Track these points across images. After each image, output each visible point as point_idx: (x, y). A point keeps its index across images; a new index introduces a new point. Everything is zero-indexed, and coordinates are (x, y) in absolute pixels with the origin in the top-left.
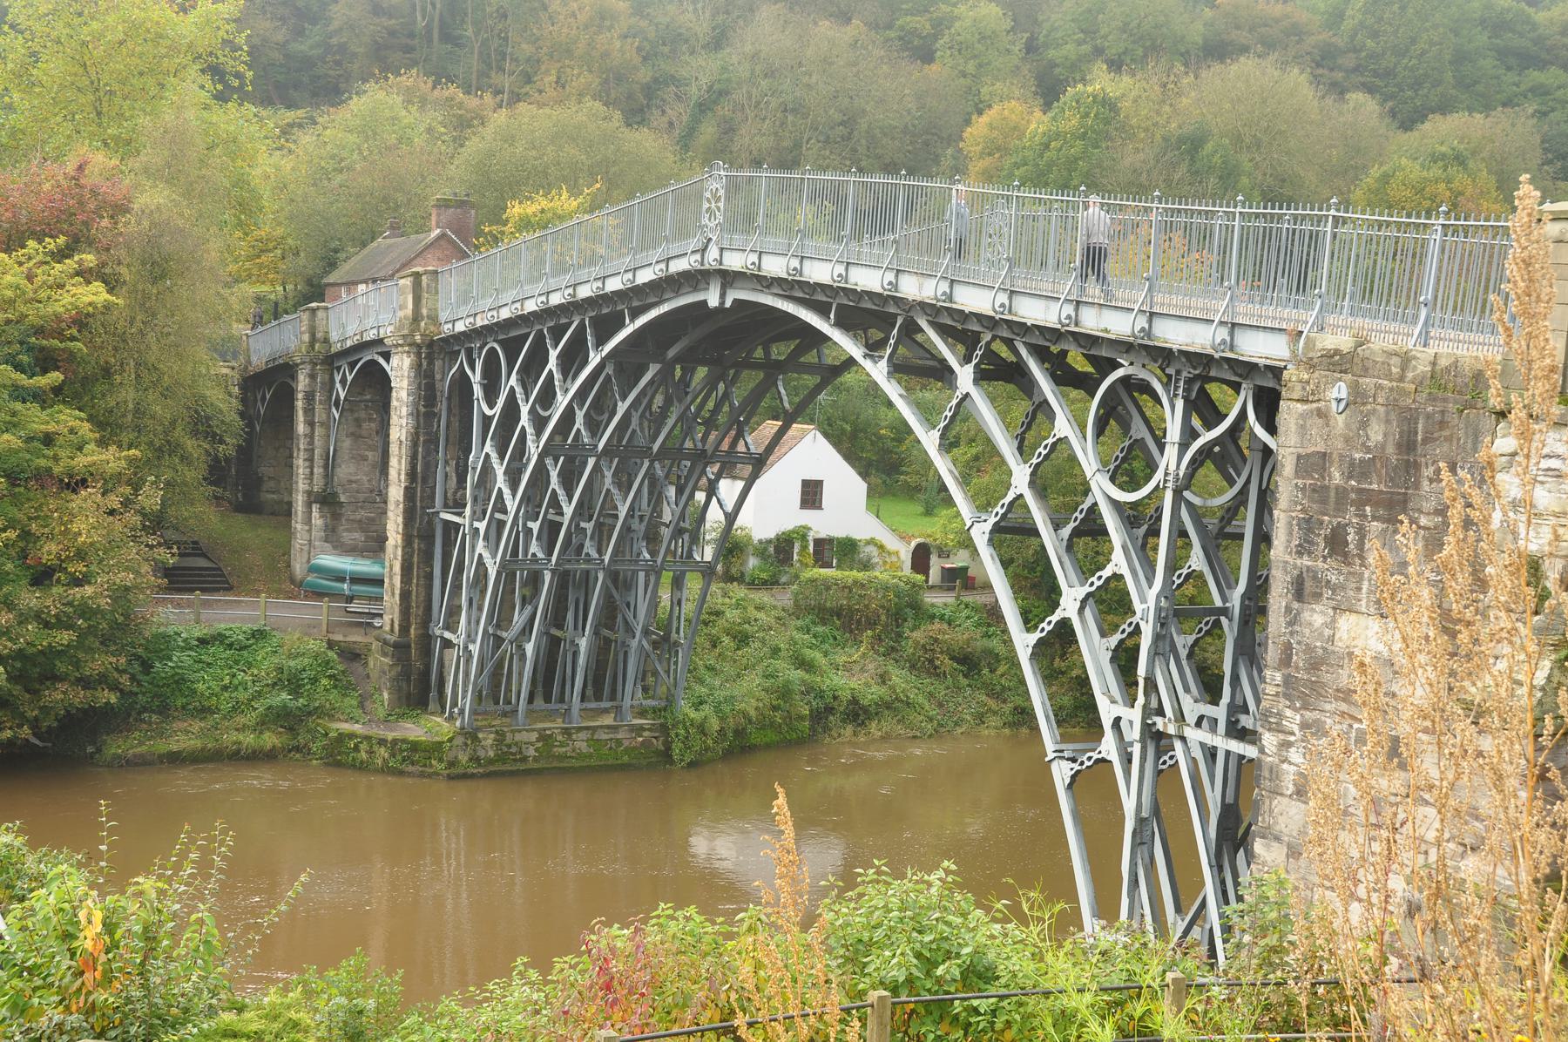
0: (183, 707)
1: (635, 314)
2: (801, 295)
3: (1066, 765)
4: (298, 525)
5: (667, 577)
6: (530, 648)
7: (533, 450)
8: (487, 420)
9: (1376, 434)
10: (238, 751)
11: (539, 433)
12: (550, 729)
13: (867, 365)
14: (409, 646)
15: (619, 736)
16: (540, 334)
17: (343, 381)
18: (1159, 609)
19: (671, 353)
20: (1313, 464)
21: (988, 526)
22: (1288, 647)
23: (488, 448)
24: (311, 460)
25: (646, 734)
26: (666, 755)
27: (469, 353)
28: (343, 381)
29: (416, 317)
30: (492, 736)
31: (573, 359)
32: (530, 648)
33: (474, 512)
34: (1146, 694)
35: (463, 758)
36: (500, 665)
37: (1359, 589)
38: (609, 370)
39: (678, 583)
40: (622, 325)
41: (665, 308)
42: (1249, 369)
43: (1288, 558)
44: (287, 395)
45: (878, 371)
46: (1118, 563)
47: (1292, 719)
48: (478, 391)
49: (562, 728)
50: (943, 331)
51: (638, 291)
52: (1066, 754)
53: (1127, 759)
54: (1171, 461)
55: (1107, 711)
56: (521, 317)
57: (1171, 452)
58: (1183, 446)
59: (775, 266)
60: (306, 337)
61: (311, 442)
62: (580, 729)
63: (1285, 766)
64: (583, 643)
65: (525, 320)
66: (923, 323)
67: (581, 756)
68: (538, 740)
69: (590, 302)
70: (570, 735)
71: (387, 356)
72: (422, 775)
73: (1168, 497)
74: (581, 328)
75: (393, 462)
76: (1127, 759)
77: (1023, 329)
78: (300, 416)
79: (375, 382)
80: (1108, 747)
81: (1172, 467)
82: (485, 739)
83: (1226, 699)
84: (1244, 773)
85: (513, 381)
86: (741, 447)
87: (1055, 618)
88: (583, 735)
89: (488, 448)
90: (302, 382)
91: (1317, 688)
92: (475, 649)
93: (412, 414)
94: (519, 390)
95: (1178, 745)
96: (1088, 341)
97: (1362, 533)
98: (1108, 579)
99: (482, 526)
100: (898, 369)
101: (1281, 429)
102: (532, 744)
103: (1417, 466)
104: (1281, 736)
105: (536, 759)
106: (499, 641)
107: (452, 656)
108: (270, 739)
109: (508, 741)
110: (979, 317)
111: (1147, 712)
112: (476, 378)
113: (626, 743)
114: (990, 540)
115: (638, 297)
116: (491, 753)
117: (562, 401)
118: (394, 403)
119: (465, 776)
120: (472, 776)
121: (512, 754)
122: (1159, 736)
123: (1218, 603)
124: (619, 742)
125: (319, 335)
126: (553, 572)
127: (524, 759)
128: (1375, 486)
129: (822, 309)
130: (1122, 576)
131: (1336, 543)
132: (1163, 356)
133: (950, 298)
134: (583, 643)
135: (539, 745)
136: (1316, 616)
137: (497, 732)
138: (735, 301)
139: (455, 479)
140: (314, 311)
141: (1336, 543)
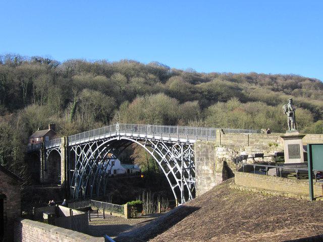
1: (105, 141)
8: (78, 157)
17: (48, 153)
47: (199, 177)
48: (76, 152)
51: (106, 138)
53: (181, 186)
55: (177, 180)
65: (86, 143)
69: (98, 140)
76: (181, 186)
80: (178, 184)
85: (83, 151)
89: (79, 160)
91: (201, 174)
100: (146, 145)
117: (92, 153)
129: (135, 139)
141: (201, 160)
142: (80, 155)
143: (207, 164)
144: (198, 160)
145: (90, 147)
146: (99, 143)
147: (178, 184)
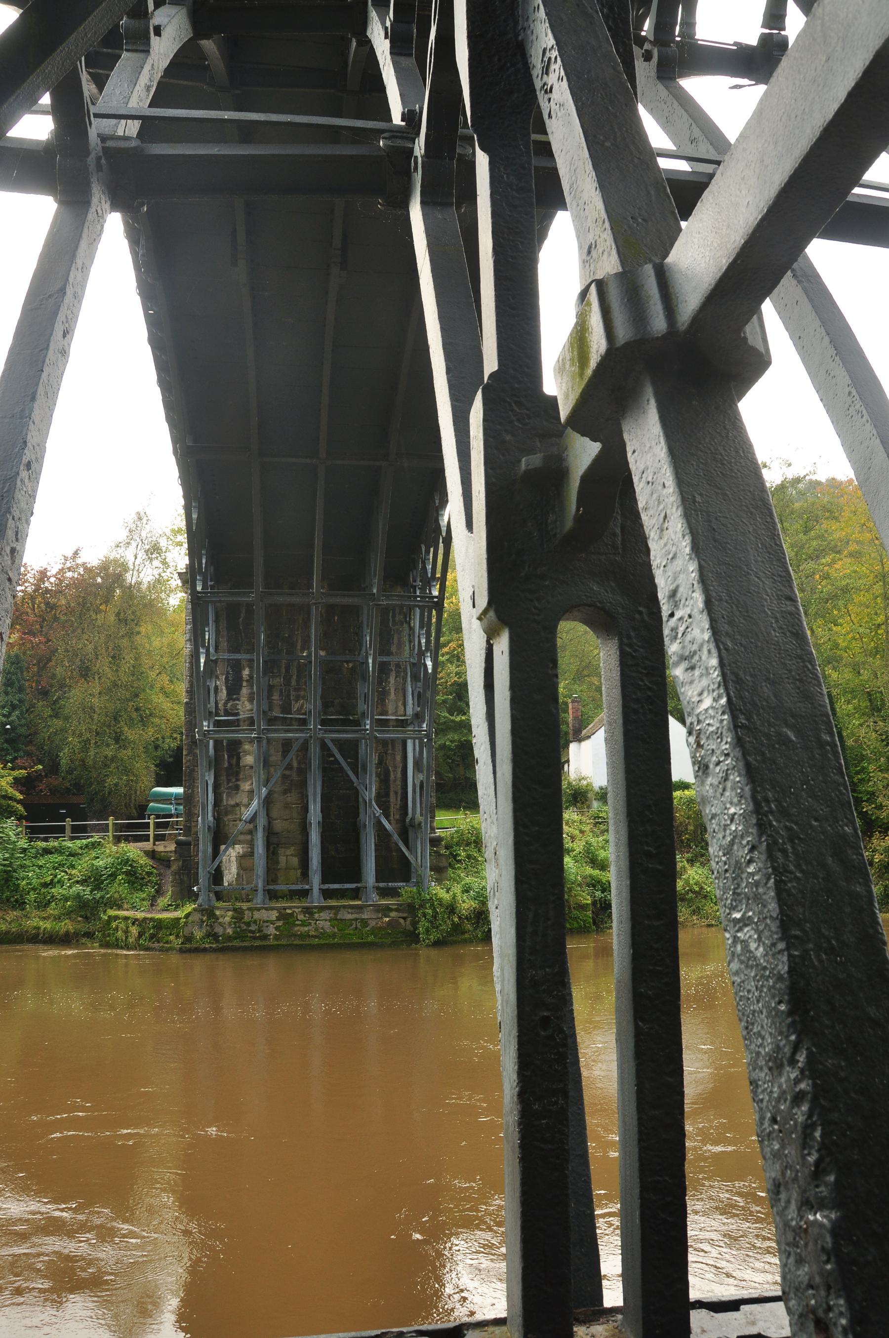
0: (8, 900)
10: (37, 935)
12: (290, 908)
15: (365, 916)
25: (393, 914)
26: (413, 937)
30: (230, 913)
35: (198, 934)
49: (303, 908)
62: (322, 909)
67: (322, 935)
68: (278, 919)
70: (311, 914)
72: (161, 950)
82: (223, 916)
88: (325, 915)
93: (190, 640)
102: (272, 923)
105: (276, 937)
108: (67, 926)
109: (246, 919)
113: (372, 923)
116: (230, 931)
119: (197, 950)
120: (205, 950)
121: (251, 932)
124: (364, 923)
127: (265, 937)
135: (280, 923)
137: (235, 910)
139: (225, 692)
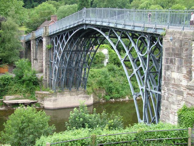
1: (74, 31)
2: (96, 27)
3: (135, 96)
4: (32, 63)
5: (83, 69)
6: (63, 80)
7: (62, 51)
9: (176, 44)
11: (63, 49)
13: (106, 37)
14: (47, 80)
16: (62, 35)
17: (37, 42)
18: (147, 72)
19: (80, 36)
20: (167, 49)
21: (123, 60)
22: (165, 77)
23: (56, 51)
24: (33, 53)
27: (53, 37)
28: (37, 42)
29: (46, 33)
31: (67, 38)
32: (63, 80)
33: (55, 61)
34: (146, 85)
36: (59, 83)
37: (175, 68)
38: (72, 39)
39: (85, 70)
40: (73, 33)
41: (78, 30)
42: (159, 35)
43: (165, 64)
44: (30, 45)
45: (107, 38)
46: (141, 65)
48: (54, 43)
50: (116, 31)
51: (74, 27)
52: (135, 94)
54: (148, 50)
56: (59, 32)
57: (148, 48)
58: (150, 47)
59: (92, 23)
60: (32, 36)
61: (33, 51)
63: (165, 96)
64: (71, 79)
66: (113, 30)
69: (68, 29)
71: (42, 38)
73: (148, 55)
74: (67, 34)
75: (44, 54)
77: (127, 31)
78: (32, 47)
79: (41, 41)
80: (141, 93)
81: (148, 50)
83: (158, 85)
84: (160, 96)
86: (93, 50)
87: (133, 74)
90: (32, 43)
92: (56, 80)
94: (60, 43)
95: (151, 93)
96: (136, 32)
97: (175, 59)
98: (140, 68)
99: (56, 62)
100: (110, 37)
101: (163, 44)
103: (182, 49)
104: (164, 91)
106: (59, 79)
107: (52, 81)
110: (120, 29)
111: (146, 88)
112: (54, 41)
114: (124, 62)
115: (75, 28)
117: (66, 44)
118: (43, 45)
122: (148, 91)
123: (157, 71)
125: (34, 36)
126: (66, 69)
128: (177, 52)
129: (99, 29)
130: (142, 67)
131: (171, 61)
132: (146, 33)
133: (116, 26)
134: (71, 79)
136: (168, 73)
138: (88, 28)
140: (33, 32)
141: (171, 61)
142: (57, 44)
143: (179, 69)
144: (167, 62)
145: (64, 37)
146: (71, 33)
147: (141, 93)
